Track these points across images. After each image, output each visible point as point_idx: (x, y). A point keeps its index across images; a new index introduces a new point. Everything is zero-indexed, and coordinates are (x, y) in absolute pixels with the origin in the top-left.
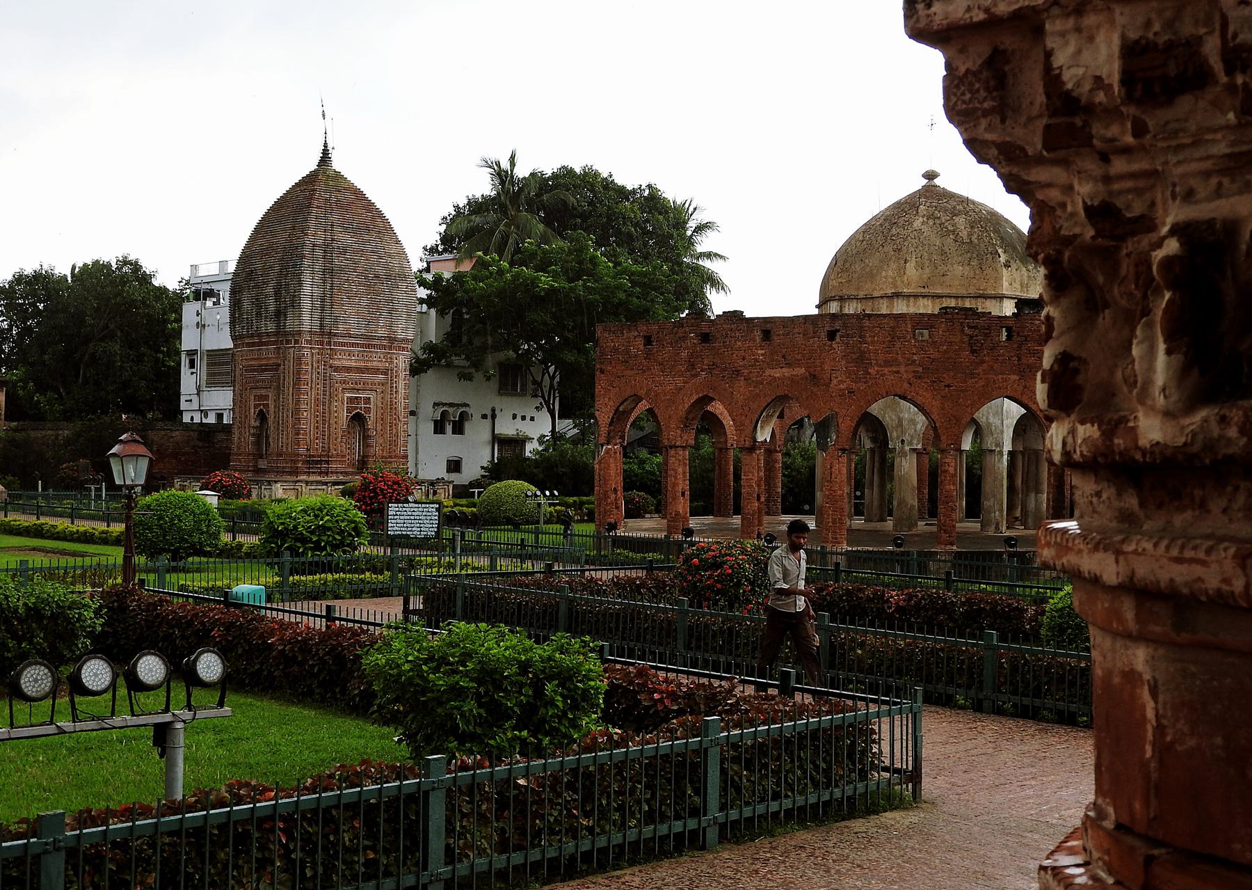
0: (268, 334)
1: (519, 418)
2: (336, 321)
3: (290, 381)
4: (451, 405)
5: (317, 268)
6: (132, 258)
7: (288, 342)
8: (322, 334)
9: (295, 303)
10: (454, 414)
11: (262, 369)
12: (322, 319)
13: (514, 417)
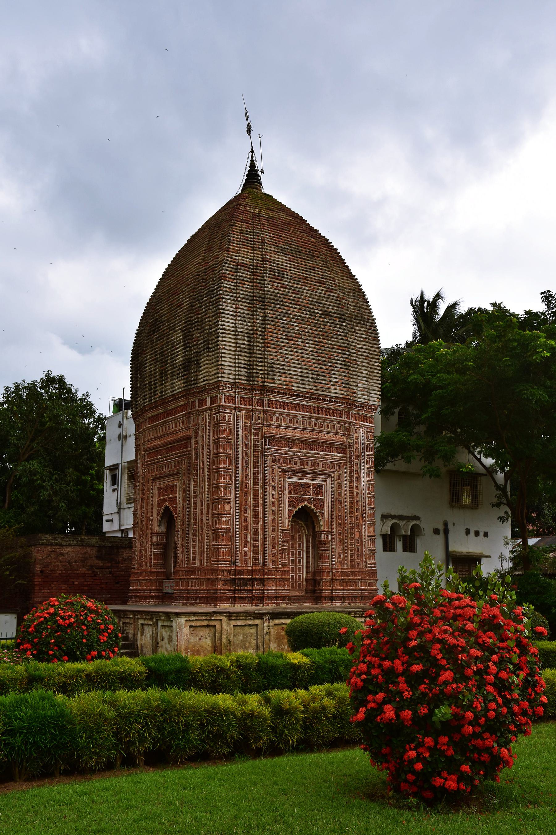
0: (175, 398)
1: (472, 534)
2: (271, 368)
3: (204, 461)
4: (401, 518)
5: (242, 294)
6: (55, 374)
7: (202, 402)
8: (251, 388)
9: (211, 344)
10: (406, 528)
11: (168, 448)
12: (250, 366)
13: (468, 532)
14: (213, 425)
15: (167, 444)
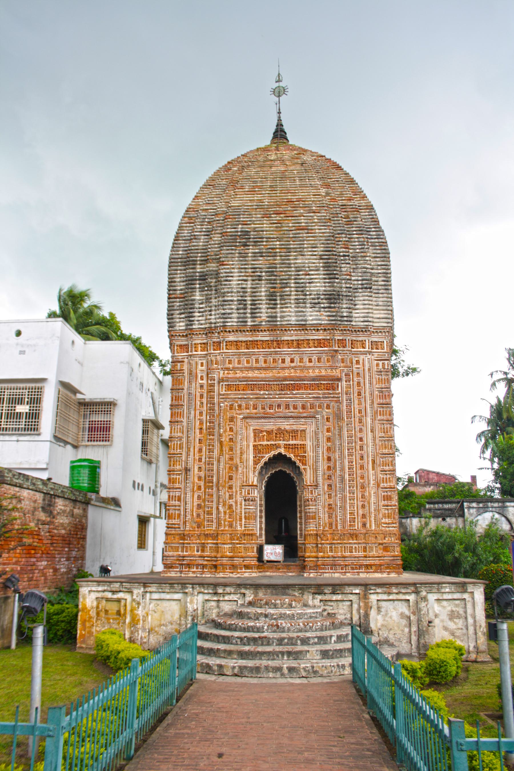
14: (377, 371)
15: (285, 379)
